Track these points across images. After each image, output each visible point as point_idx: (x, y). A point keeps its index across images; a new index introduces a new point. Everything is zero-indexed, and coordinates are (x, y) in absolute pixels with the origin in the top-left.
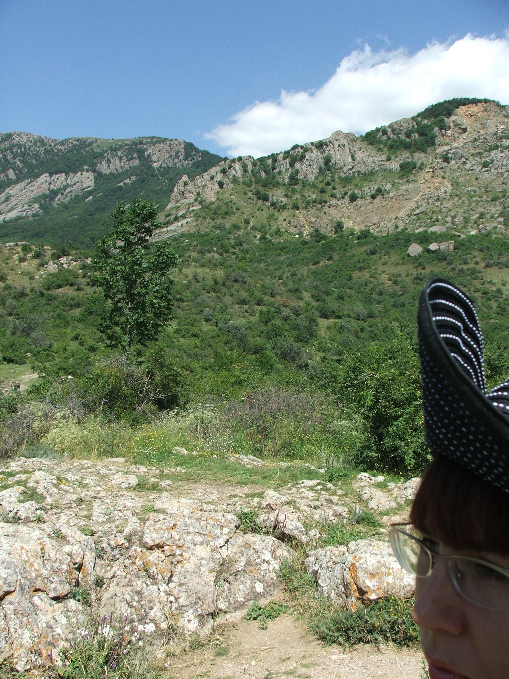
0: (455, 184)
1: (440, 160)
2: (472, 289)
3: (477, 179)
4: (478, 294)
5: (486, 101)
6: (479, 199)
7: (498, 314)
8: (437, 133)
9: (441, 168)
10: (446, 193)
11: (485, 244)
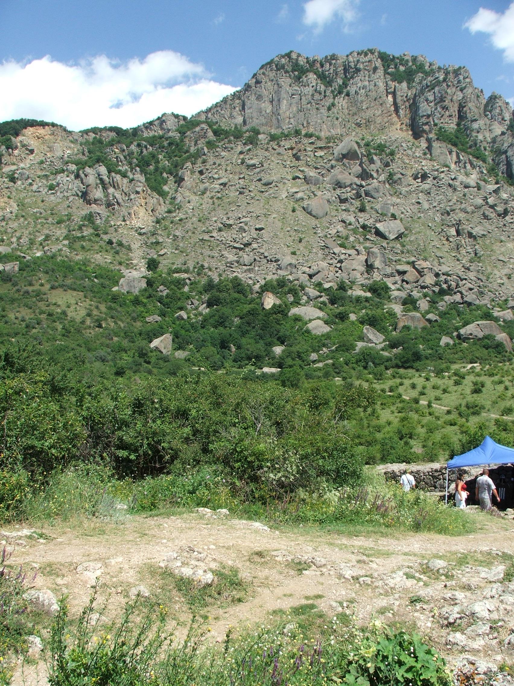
0: (21, 205)
1: (6, 180)
2: (37, 311)
3: (43, 201)
4: (43, 316)
5: (53, 125)
6: (45, 221)
7: (64, 335)
8: (4, 152)
9: (7, 188)
10: (11, 213)
11: (50, 266)
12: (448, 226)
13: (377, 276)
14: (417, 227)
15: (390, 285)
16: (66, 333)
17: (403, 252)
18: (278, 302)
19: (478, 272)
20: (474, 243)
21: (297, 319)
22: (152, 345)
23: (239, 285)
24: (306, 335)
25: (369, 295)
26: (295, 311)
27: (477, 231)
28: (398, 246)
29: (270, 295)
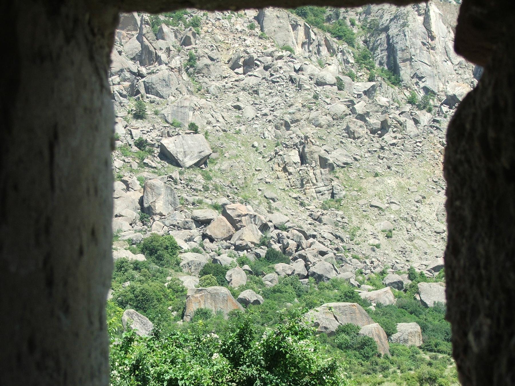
12: (287, 146)
13: (157, 228)
14: (232, 148)
15: (180, 242)
17: (206, 189)
19: (336, 225)
20: (331, 176)
25: (141, 258)
27: (336, 156)
28: (200, 178)
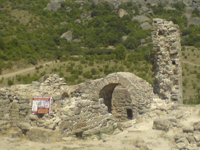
7: (17, 32)
16: (19, 31)
18: (126, 14)
21: (136, 22)
22: (62, 37)
23: (107, 5)
24: (140, 30)
25: (174, 9)
26: (135, 18)
29: (123, 10)
